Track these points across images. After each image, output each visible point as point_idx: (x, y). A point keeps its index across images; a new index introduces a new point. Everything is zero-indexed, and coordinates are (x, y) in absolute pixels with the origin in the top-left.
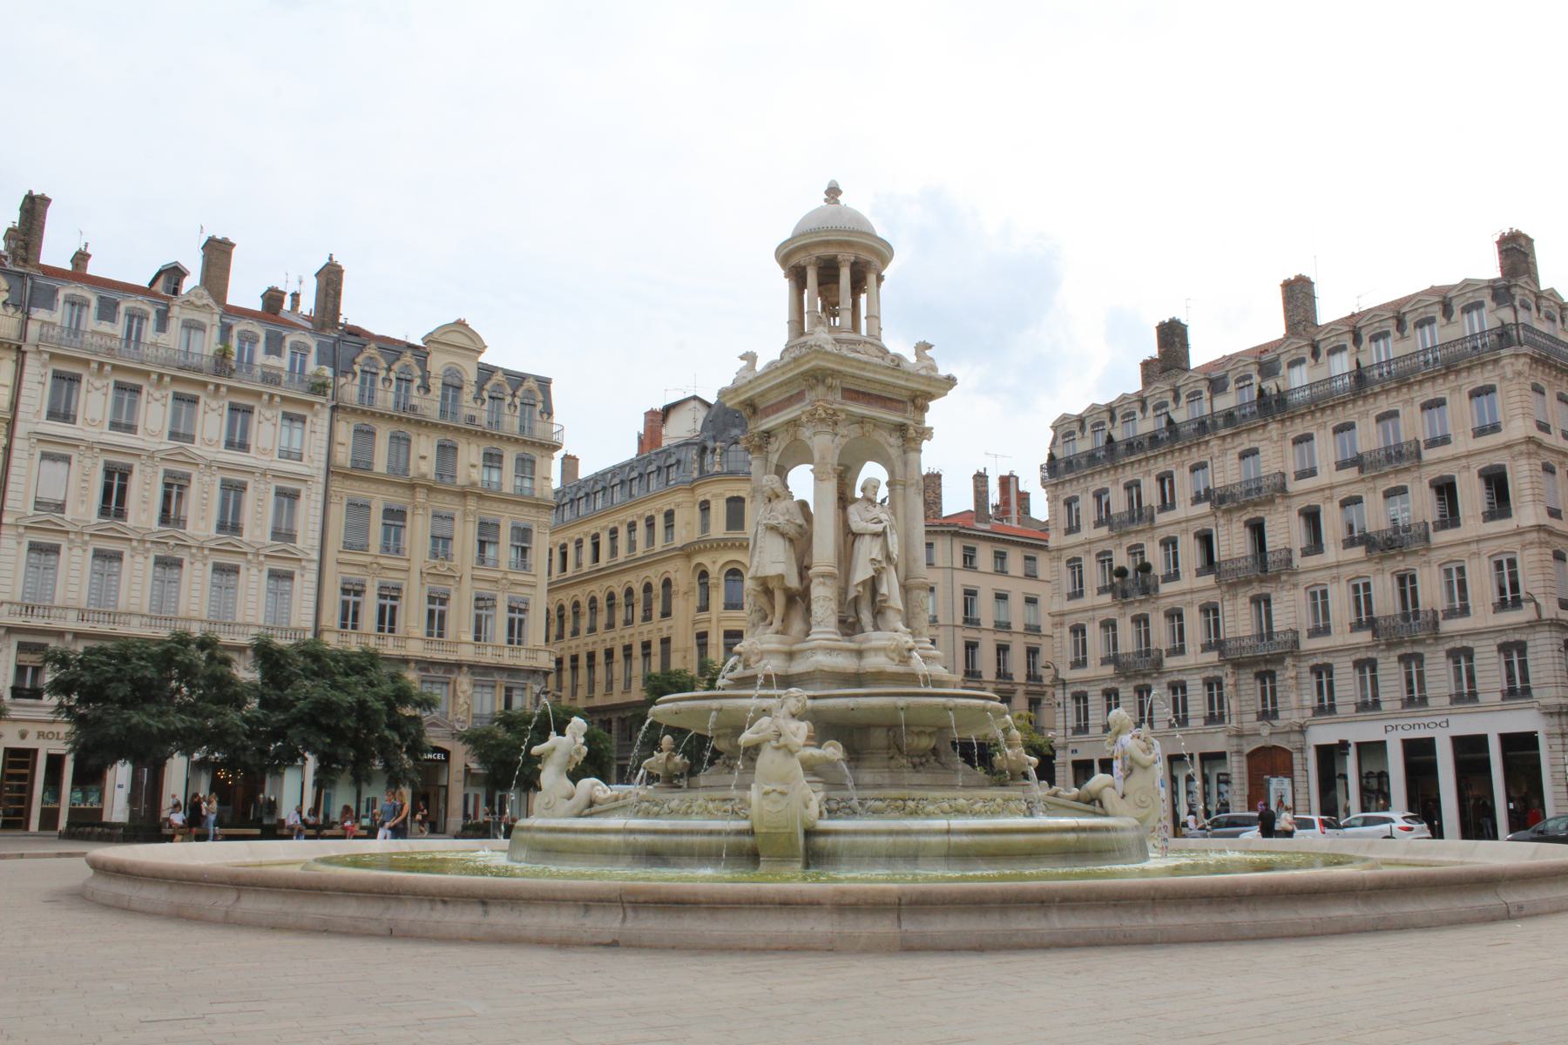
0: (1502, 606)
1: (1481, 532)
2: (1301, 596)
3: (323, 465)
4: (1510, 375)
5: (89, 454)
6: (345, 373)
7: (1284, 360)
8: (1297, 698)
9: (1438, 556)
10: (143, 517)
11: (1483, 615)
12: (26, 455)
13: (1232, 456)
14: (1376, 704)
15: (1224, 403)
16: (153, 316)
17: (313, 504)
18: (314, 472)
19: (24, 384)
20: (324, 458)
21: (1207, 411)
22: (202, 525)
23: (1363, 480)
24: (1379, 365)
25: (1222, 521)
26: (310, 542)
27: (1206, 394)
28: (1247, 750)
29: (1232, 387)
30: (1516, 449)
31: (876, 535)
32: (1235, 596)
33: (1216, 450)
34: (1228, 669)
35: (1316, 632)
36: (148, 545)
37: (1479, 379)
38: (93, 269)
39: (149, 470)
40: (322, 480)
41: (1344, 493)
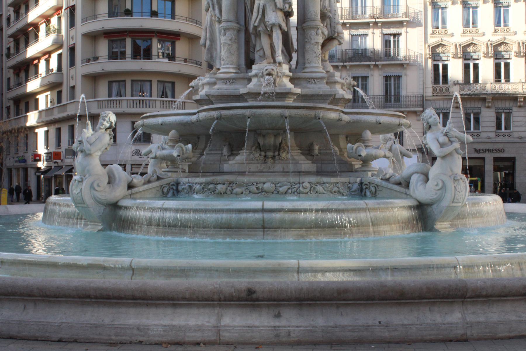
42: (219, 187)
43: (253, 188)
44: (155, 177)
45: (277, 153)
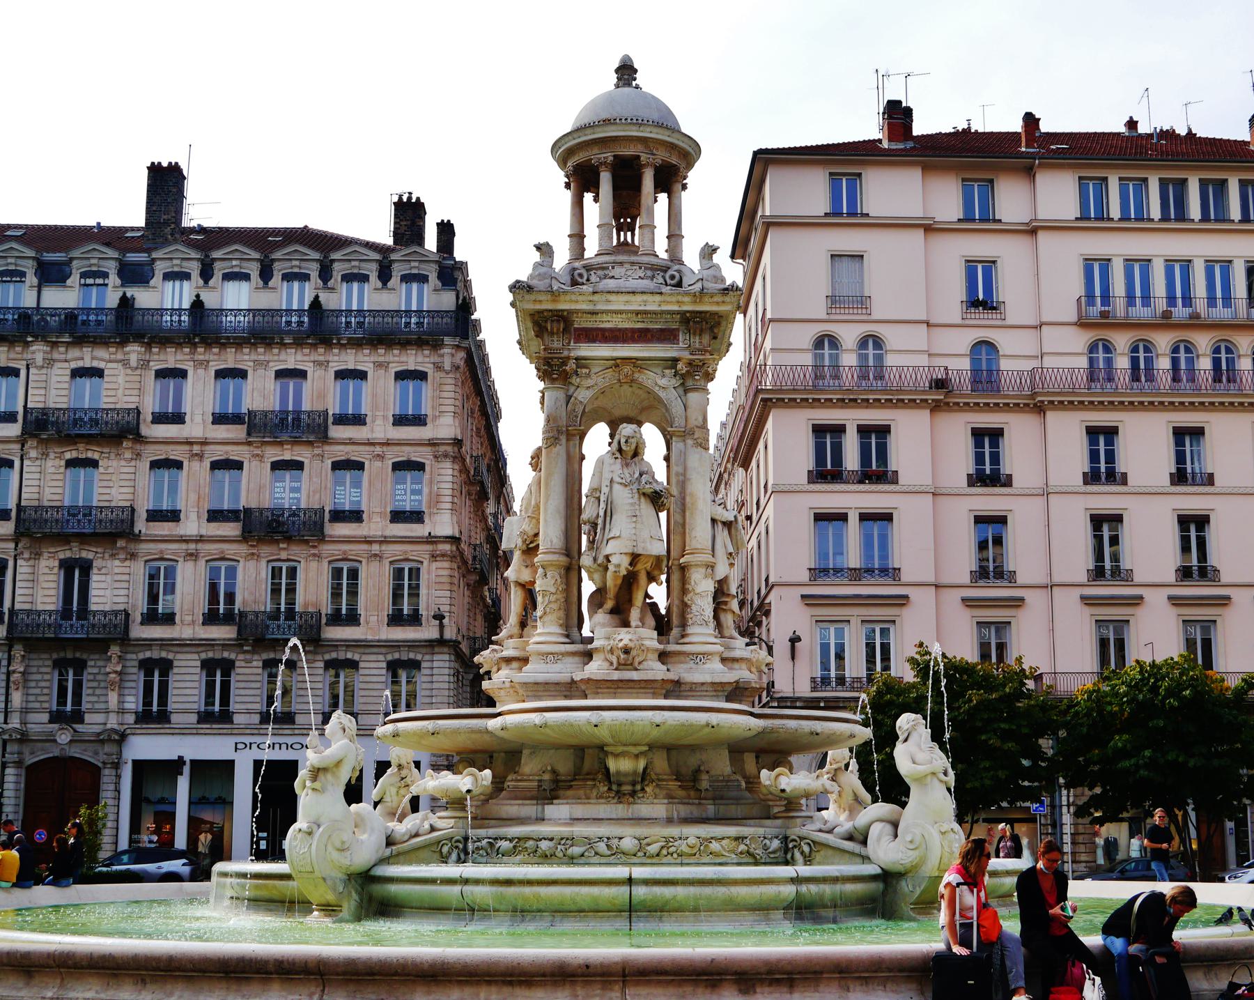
0: (396, 619)
1: (388, 533)
2: (139, 570)
4: (447, 366)
7: (161, 268)
8: (110, 702)
9: (328, 549)
11: (373, 624)
13: (60, 374)
14: (225, 717)
15: (60, 298)
21: (29, 300)
23: (249, 443)
24: (289, 311)
25: (33, 454)
27: (32, 279)
28: (30, 760)
29: (74, 280)
30: (442, 449)
31: (724, 523)
32: (37, 556)
33: (39, 358)
34: (18, 651)
35: (151, 617)
37: (412, 359)
41: (219, 453)
42: (544, 845)
43: (602, 847)
44: (427, 826)
45: (638, 787)
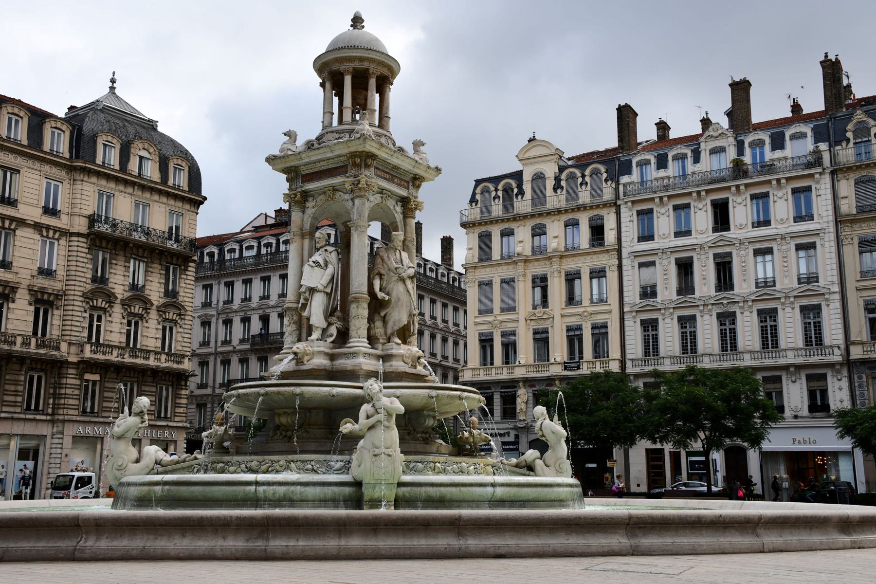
3: (831, 218)
5: (664, 257)
6: (838, 143)
10: (705, 289)
12: (630, 267)
16: (689, 154)
17: (827, 250)
18: (824, 225)
19: (622, 225)
20: (831, 213)
22: (745, 285)
26: (830, 279)
36: (710, 307)
38: (673, 135)
39: (703, 257)
40: (832, 229)
